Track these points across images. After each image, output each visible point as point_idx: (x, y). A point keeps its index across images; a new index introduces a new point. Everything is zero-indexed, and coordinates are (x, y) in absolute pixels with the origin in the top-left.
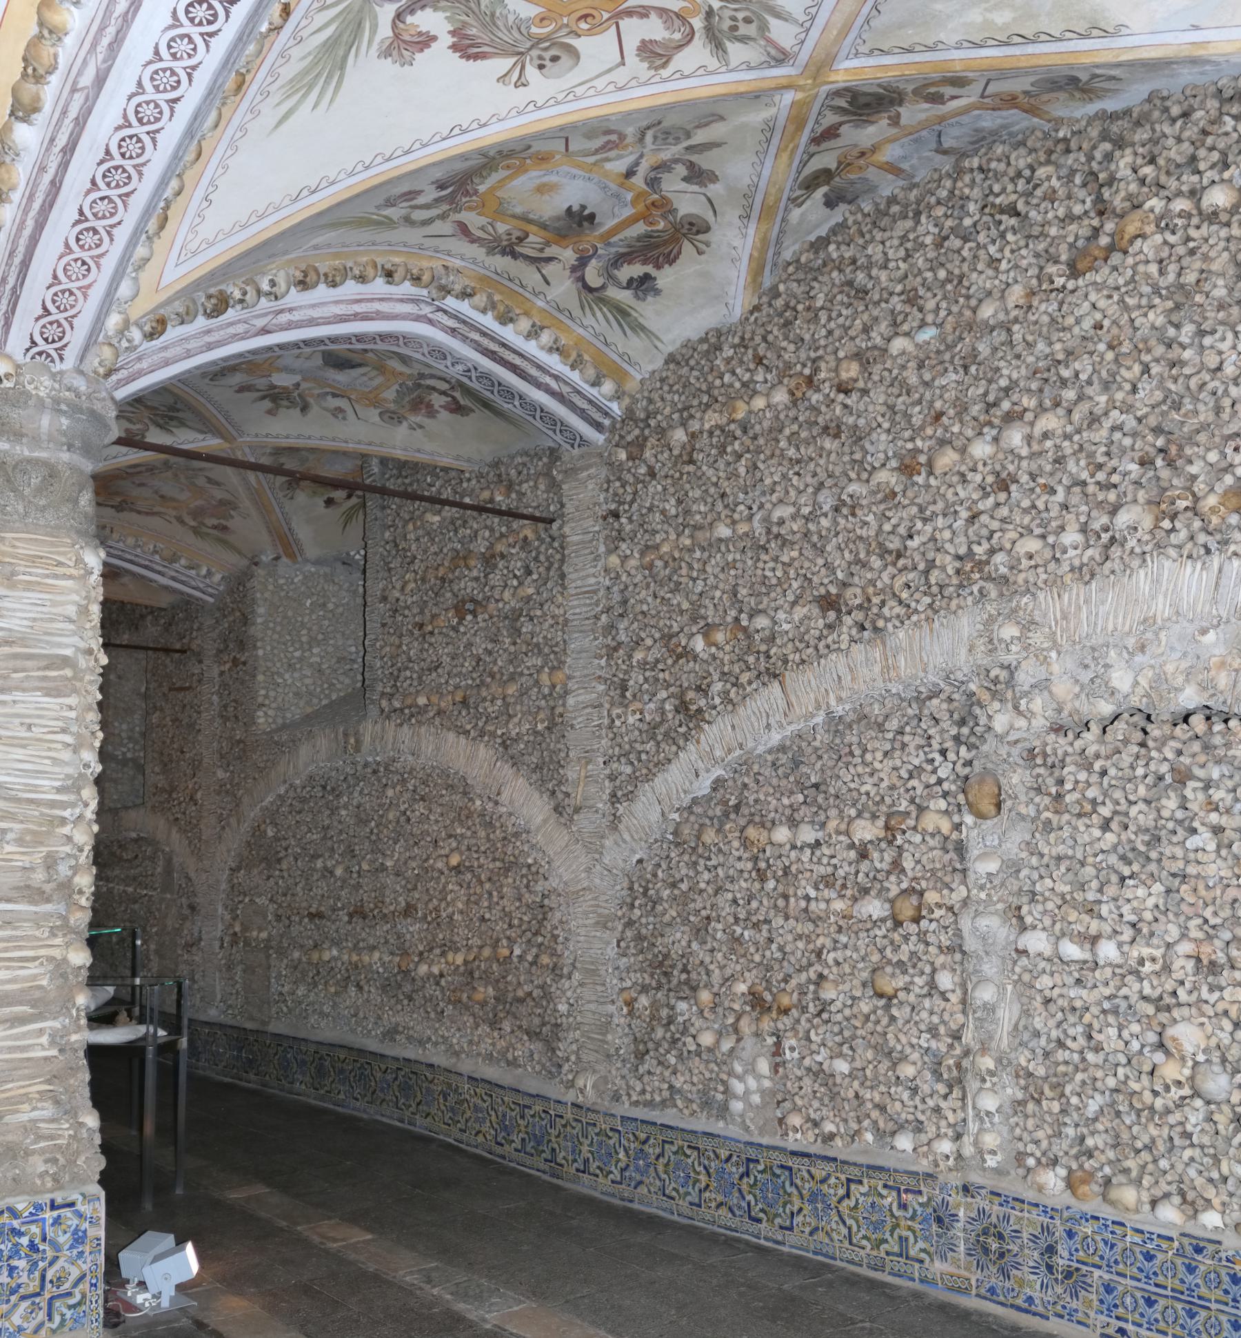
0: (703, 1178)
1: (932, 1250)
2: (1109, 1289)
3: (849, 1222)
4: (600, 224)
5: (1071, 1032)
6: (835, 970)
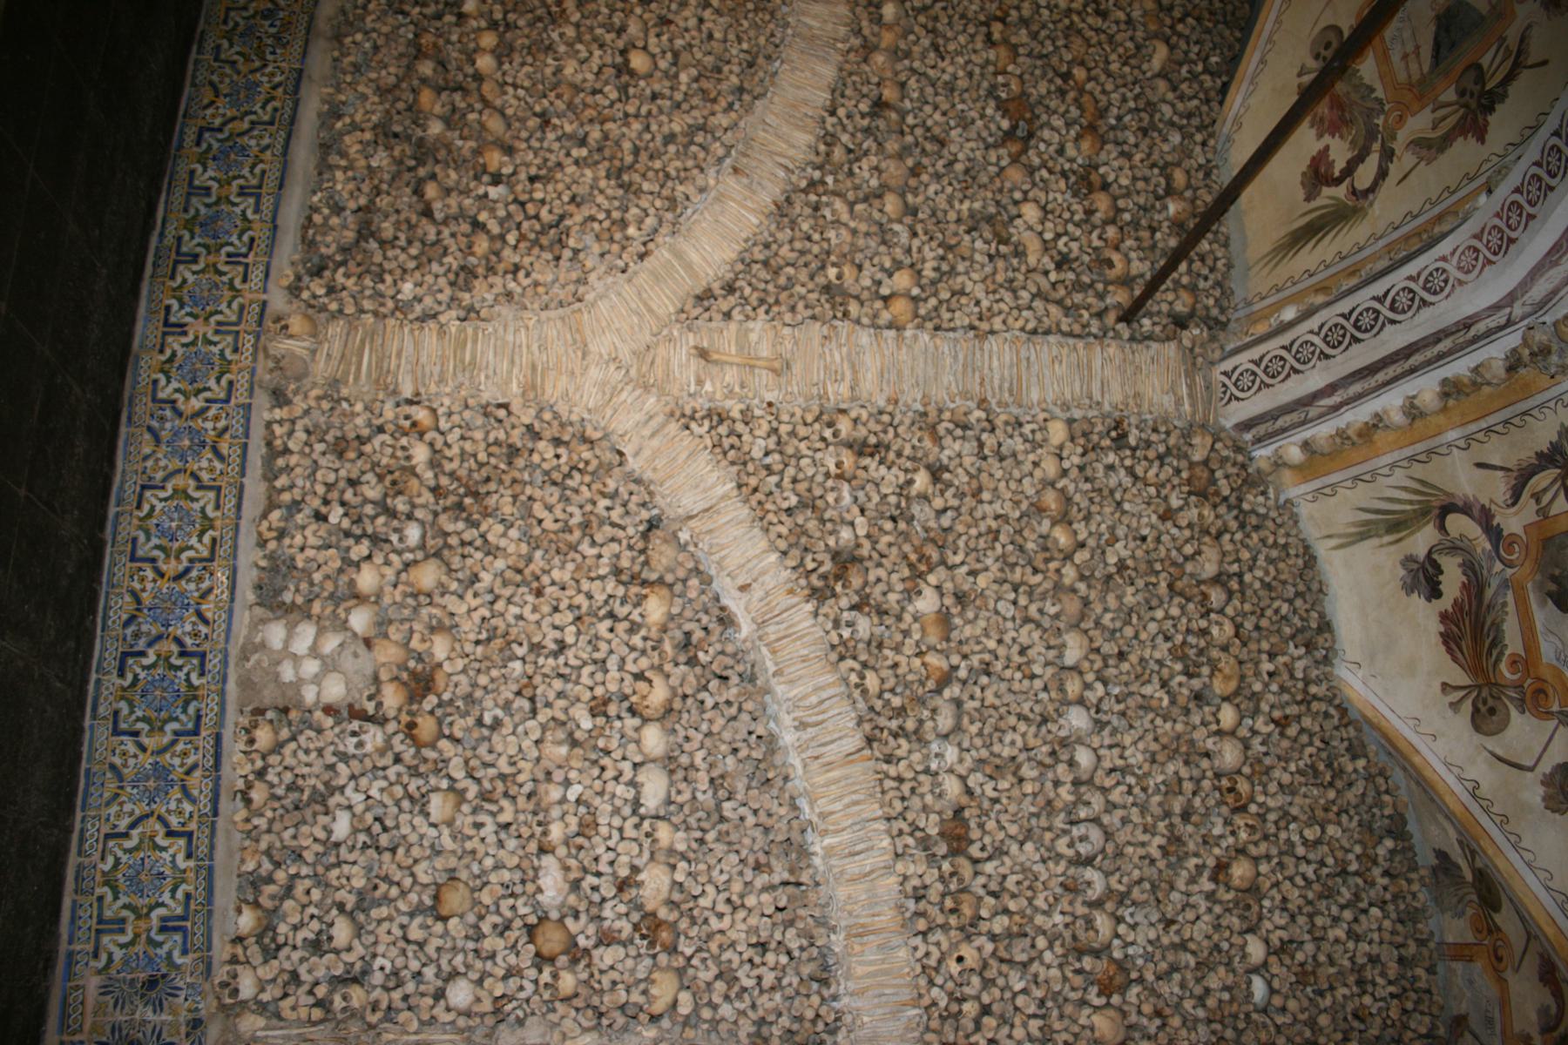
0: (171, 567)
1: (113, 972)
3: (135, 832)
4: (1543, 604)
6: (470, 819)
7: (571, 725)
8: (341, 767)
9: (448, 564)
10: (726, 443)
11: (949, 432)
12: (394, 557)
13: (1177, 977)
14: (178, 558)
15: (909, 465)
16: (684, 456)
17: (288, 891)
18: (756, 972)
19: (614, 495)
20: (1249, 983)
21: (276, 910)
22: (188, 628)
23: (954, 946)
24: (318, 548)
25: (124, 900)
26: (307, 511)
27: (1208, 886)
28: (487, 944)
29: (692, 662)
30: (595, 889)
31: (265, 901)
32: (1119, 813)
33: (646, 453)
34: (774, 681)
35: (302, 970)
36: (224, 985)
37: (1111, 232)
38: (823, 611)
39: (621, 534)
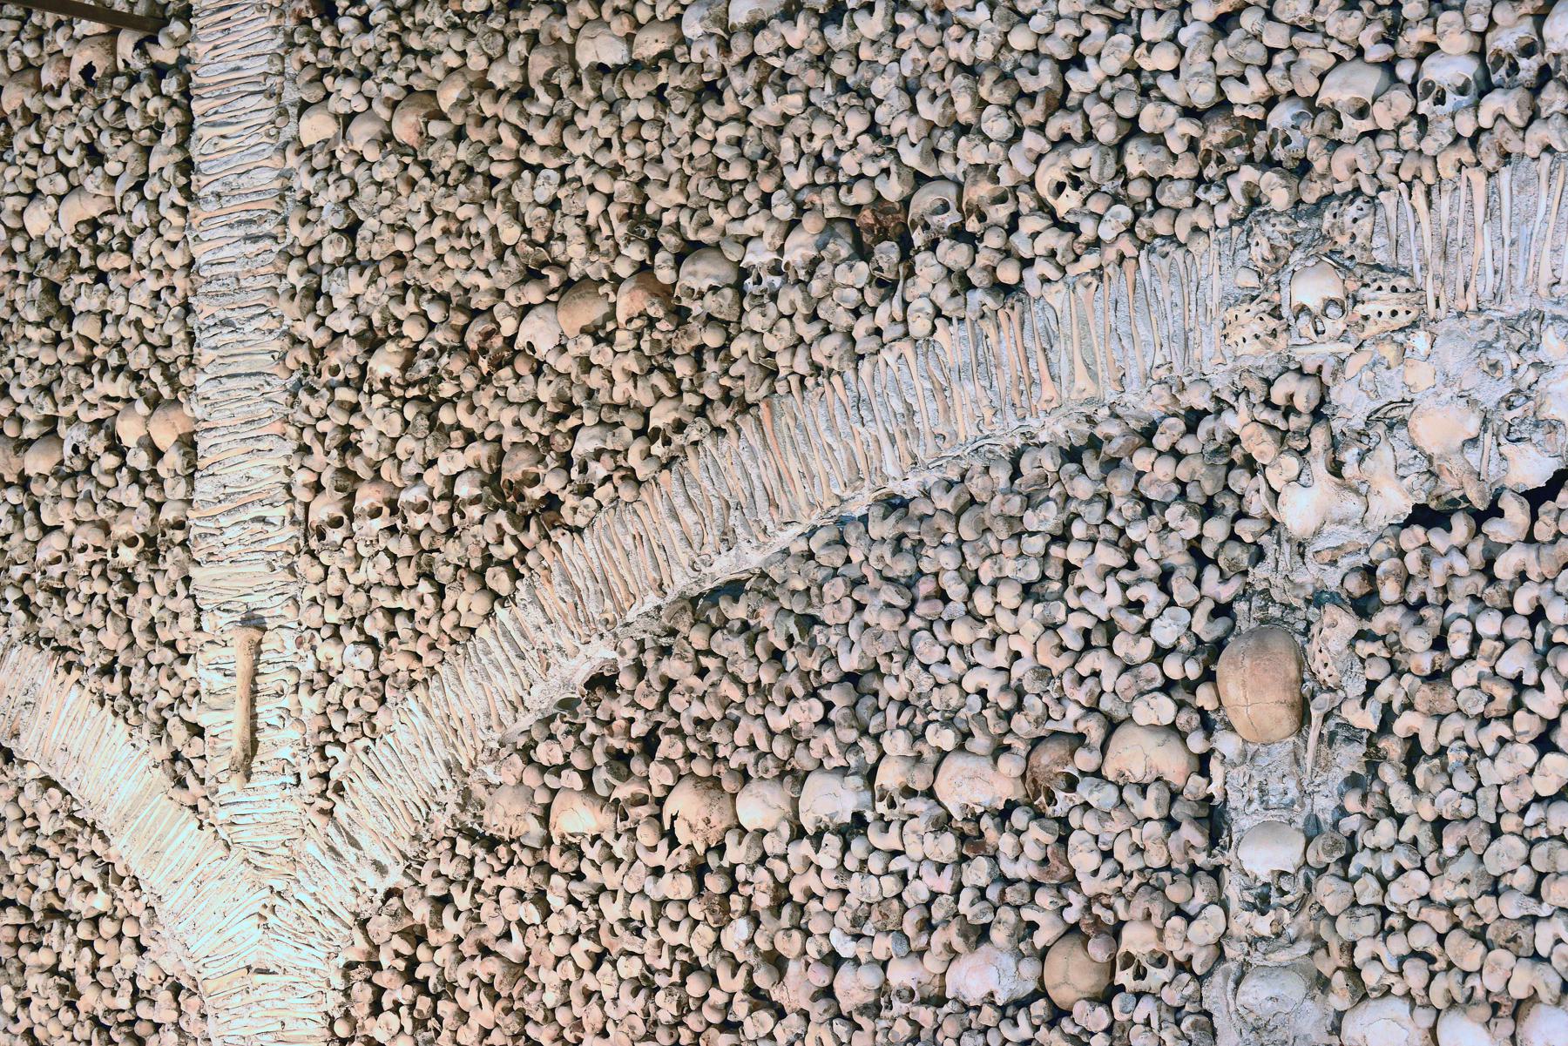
11: (321, 324)
16: (373, 785)
23: (1044, 207)
29: (649, 744)
30: (982, 893)
37: (49, 77)
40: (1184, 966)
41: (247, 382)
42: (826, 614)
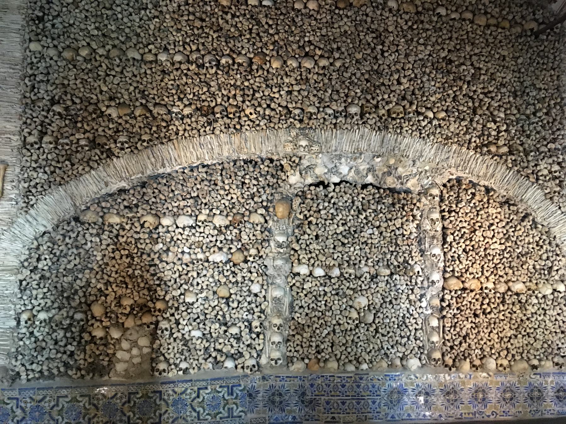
0: (93, 412)
1: (246, 410)
2: (328, 403)
3: (197, 410)
5: (319, 304)
6: (195, 287)
7: (161, 252)
8: (175, 336)
9: (93, 301)
10: (40, 189)
11: (35, 95)
12: (90, 323)
13: (261, 34)
14: (88, 410)
15: (51, 113)
16: (46, 207)
17: (219, 351)
18: (252, 187)
19: (64, 236)
20: (265, 6)
21: (226, 354)
22: (118, 401)
23: (246, 116)
24: (85, 353)
25: (221, 410)
26: (69, 360)
27: (229, 17)
28: (240, 279)
29: (137, 206)
30: (221, 242)
31: (222, 359)
32: (201, 47)
33: (44, 222)
34: (145, 175)
35: (247, 343)
36: (251, 370)
38: (117, 155)
39: (82, 233)
40: (261, 257)
41: (7, 104)
42: (189, 185)
